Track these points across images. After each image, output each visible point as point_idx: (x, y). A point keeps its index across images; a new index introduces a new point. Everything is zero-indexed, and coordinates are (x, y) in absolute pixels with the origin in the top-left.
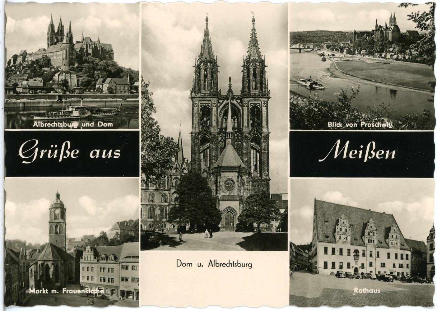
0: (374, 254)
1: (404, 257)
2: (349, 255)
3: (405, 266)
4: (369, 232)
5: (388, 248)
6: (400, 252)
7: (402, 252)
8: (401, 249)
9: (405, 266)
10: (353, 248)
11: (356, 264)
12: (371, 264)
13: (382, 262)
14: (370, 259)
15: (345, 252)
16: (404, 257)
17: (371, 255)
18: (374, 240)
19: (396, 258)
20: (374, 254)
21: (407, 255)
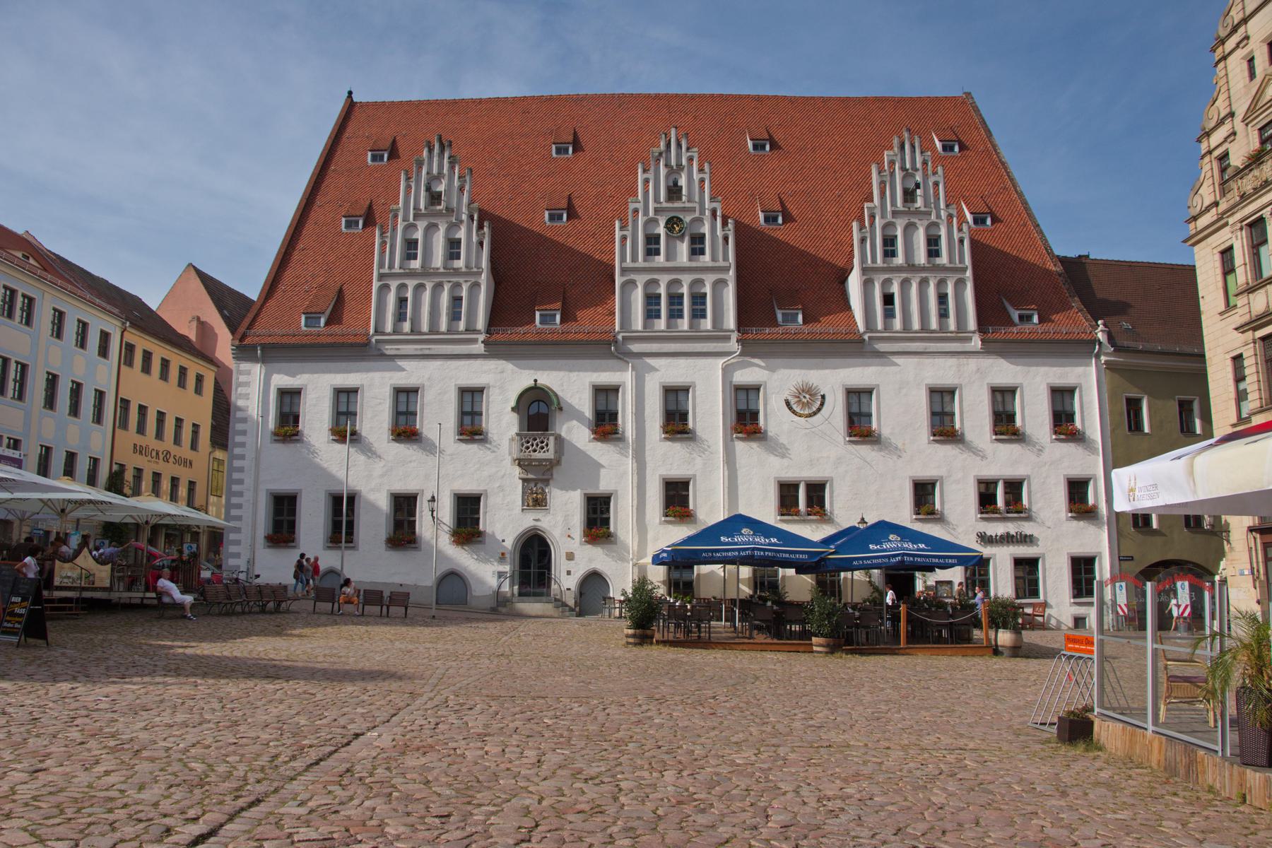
0: (710, 413)
1: (1034, 413)
2: (471, 428)
3: (1048, 499)
4: (652, 240)
5: (854, 346)
6: (976, 377)
7: (1003, 371)
8: (992, 347)
9: (1048, 499)
10: (506, 382)
11: (536, 500)
12: (677, 496)
13: (790, 475)
14: (669, 459)
15: (439, 417)
16: (1034, 413)
17: (677, 422)
18: (698, 299)
19: (944, 428)
20: (710, 413)
21: (1062, 397)
